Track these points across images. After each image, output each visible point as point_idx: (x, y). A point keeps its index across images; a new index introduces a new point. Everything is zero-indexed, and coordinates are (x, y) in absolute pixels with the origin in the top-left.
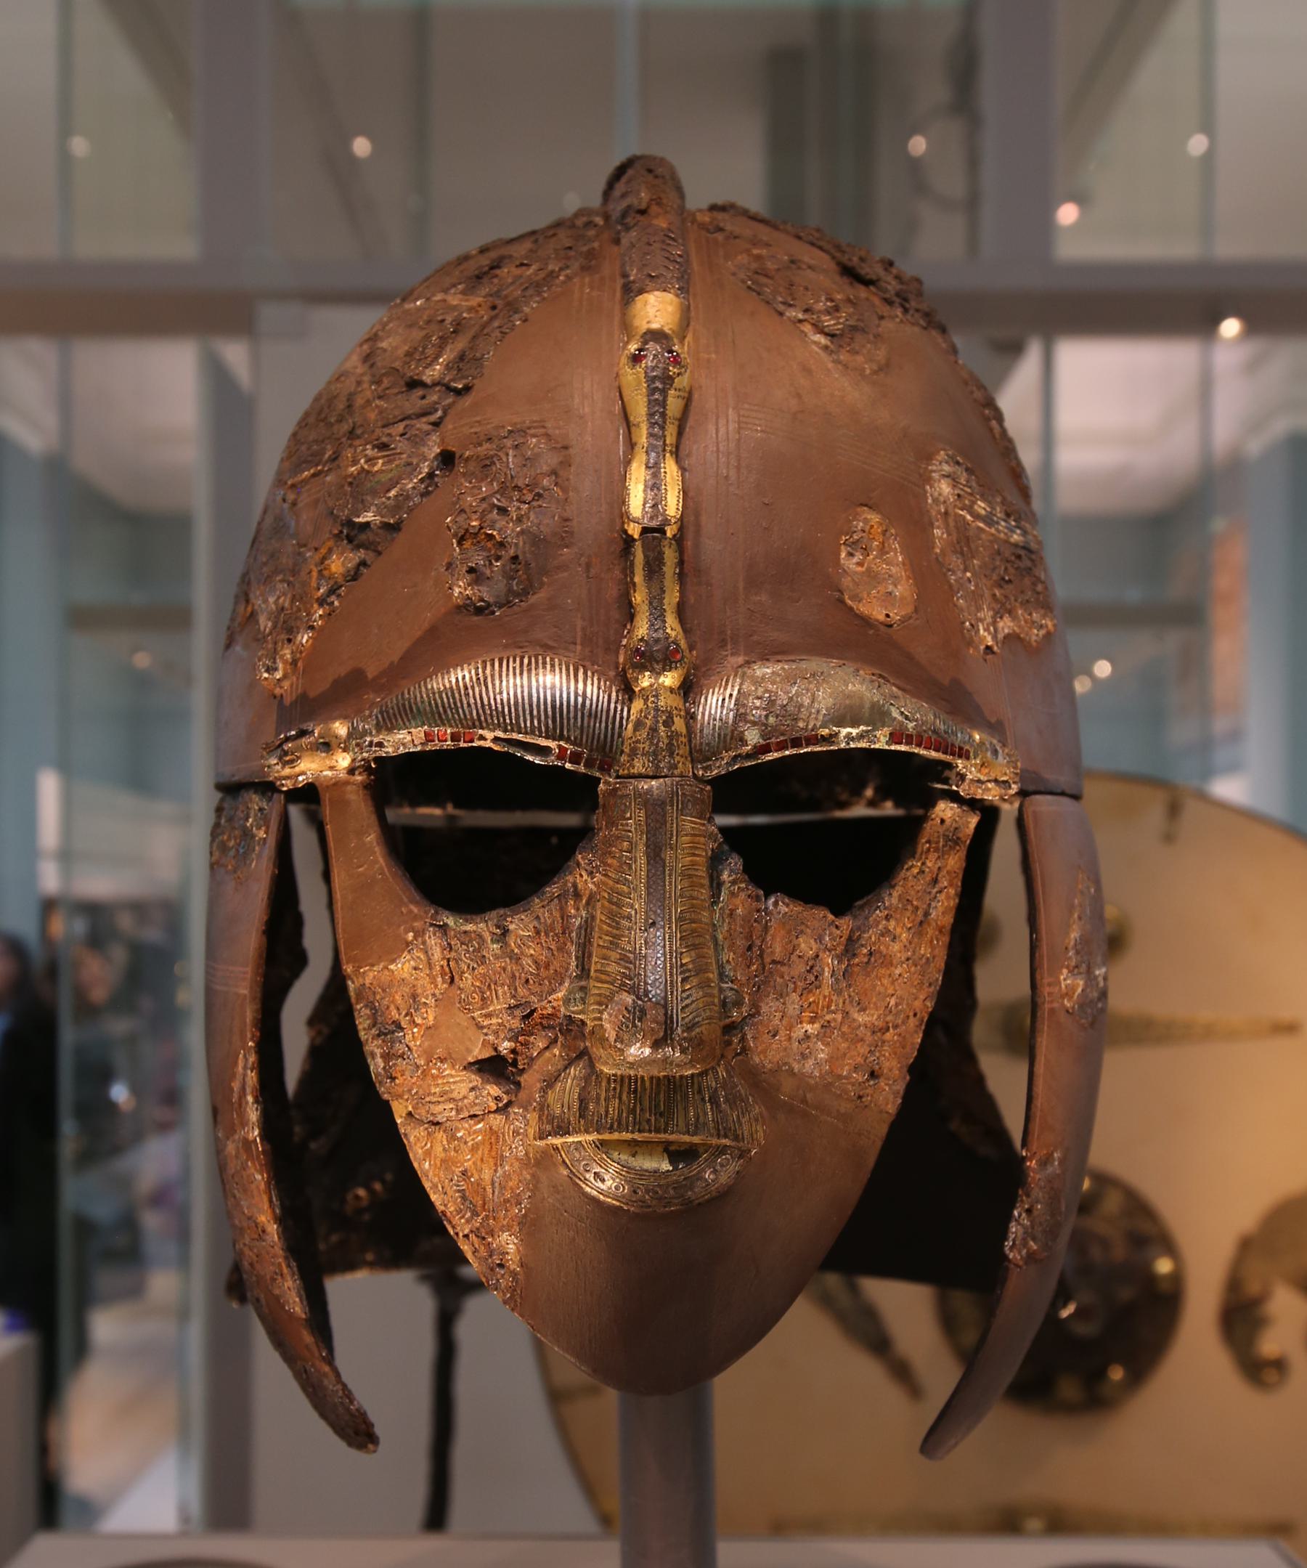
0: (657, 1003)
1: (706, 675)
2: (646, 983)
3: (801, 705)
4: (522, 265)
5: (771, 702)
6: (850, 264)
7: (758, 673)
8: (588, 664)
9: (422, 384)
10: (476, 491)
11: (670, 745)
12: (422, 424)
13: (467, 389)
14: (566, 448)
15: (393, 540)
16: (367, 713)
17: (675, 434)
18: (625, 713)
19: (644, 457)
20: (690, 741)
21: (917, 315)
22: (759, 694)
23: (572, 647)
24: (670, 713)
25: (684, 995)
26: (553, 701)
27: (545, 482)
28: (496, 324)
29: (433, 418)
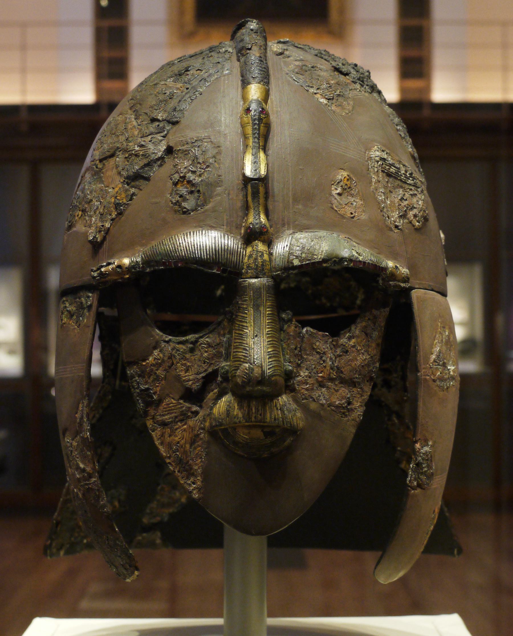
0: (258, 366)
1: (277, 238)
2: (254, 359)
3: (315, 249)
4: (198, 70)
5: (303, 248)
6: (337, 67)
7: (299, 237)
8: (229, 233)
9: (158, 120)
10: (182, 164)
11: (262, 265)
12: (159, 137)
13: (177, 122)
14: (219, 147)
15: (147, 184)
16: (137, 255)
17: (263, 142)
18: (244, 253)
19: (251, 151)
20: (271, 264)
21: (367, 87)
22: (298, 245)
23: (222, 227)
24: (263, 252)
25: (270, 363)
26: (215, 248)
27: (211, 161)
28: (188, 96)
29: (162, 134)
